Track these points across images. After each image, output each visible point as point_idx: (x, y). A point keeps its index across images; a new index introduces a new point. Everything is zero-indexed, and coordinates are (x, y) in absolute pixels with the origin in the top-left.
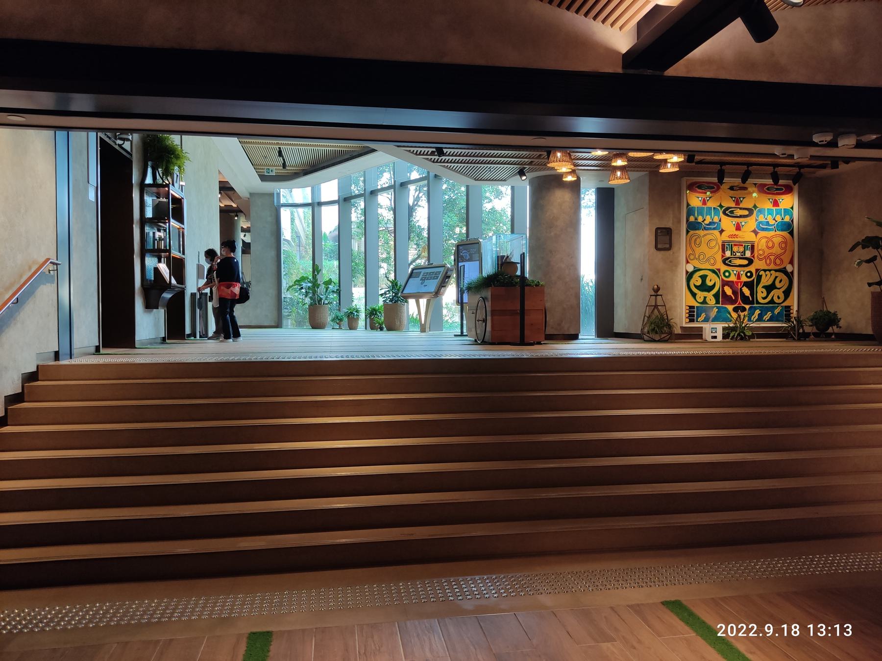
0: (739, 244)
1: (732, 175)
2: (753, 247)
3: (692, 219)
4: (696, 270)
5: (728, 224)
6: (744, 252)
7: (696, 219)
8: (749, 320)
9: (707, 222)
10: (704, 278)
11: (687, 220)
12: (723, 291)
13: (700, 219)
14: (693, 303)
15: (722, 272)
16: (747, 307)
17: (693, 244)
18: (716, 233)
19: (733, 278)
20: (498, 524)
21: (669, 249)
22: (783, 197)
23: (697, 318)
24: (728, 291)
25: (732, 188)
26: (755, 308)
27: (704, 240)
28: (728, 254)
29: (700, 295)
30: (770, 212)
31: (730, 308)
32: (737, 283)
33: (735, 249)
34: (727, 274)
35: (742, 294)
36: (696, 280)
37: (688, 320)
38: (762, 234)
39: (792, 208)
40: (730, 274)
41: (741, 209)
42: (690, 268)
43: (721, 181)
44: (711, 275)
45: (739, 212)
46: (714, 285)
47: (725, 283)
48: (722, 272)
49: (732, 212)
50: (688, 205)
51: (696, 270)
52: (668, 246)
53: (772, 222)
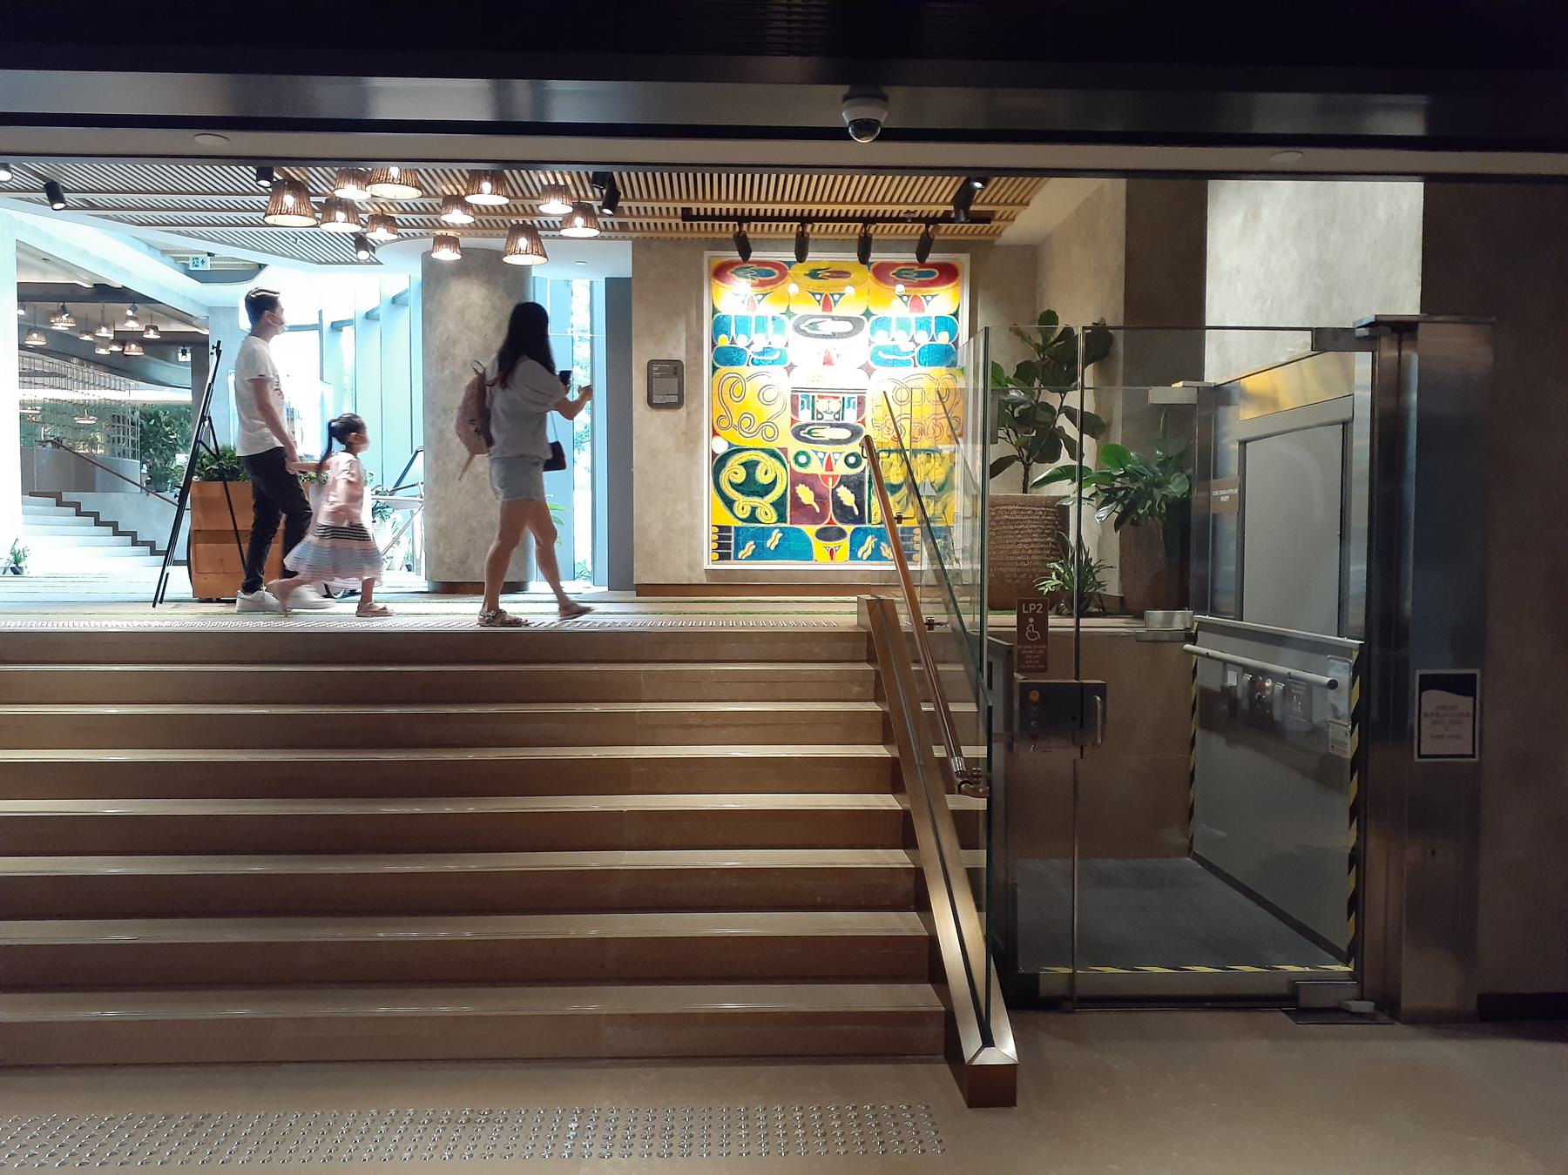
0: (833, 394)
1: (826, 245)
2: (861, 403)
3: (723, 341)
4: (734, 451)
5: (805, 352)
6: (841, 413)
7: (733, 342)
8: (853, 555)
9: (757, 347)
10: (750, 466)
11: (714, 345)
12: (794, 494)
13: (741, 342)
14: (727, 519)
15: (791, 455)
16: (849, 529)
17: (726, 397)
18: (778, 370)
19: (816, 468)
20: (133, 921)
21: (678, 405)
22: (935, 290)
23: (737, 549)
24: (806, 495)
25: (814, 274)
26: (866, 532)
27: (753, 387)
28: (805, 416)
29: (744, 504)
30: (903, 324)
31: (810, 530)
32: (825, 478)
33: (821, 405)
34: (802, 459)
35: (838, 503)
36: (734, 472)
37: (716, 556)
38: (882, 372)
39: (956, 315)
40: (808, 458)
41: (833, 318)
42: (721, 447)
43: (801, 257)
44: (766, 462)
45: (828, 327)
46: (774, 482)
47: (796, 479)
48: (791, 455)
49: (813, 326)
50: (715, 311)
51: (734, 451)
52: (674, 399)
53: (907, 346)
